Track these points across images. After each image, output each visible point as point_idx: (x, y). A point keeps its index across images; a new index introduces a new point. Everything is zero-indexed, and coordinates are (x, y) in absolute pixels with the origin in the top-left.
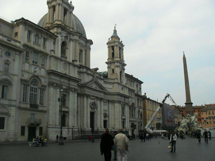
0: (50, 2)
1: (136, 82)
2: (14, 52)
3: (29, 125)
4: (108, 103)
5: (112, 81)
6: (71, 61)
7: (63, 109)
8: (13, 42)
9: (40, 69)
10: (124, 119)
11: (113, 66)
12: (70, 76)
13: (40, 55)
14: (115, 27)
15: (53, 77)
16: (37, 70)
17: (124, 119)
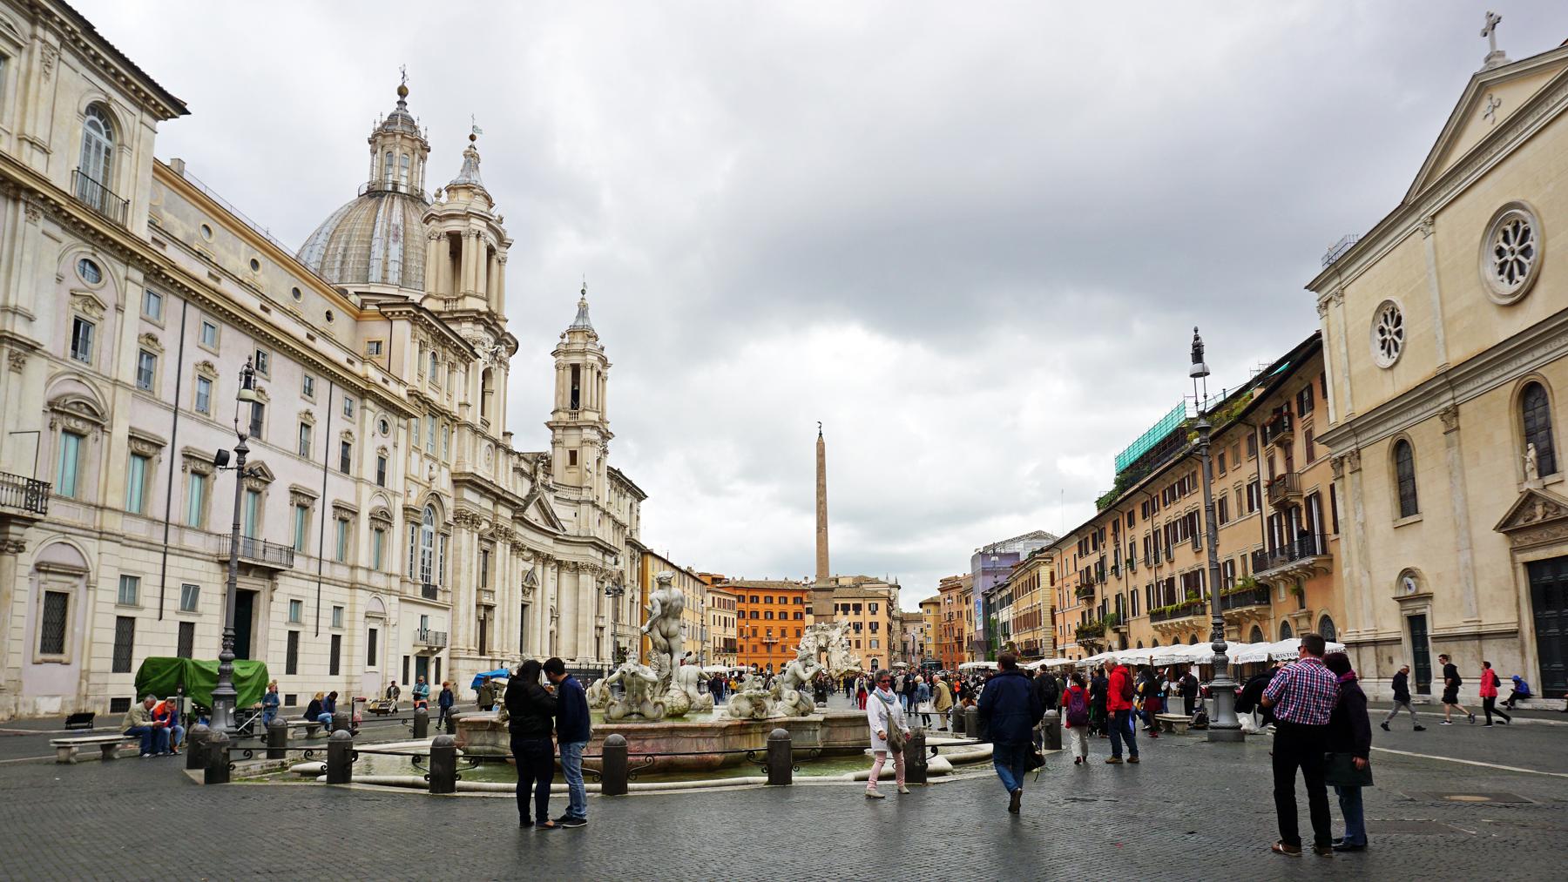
0: (440, 217)
1: (628, 495)
2: (395, 419)
3: (423, 651)
4: (556, 570)
5: (574, 497)
6: (501, 437)
7: (486, 600)
8: (392, 387)
9: (440, 470)
10: (602, 628)
11: (572, 440)
12: (504, 491)
13: (440, 420)
14: (583, 292)
15: (468, 495)
16: (435, 467)
17: (602, 628)
